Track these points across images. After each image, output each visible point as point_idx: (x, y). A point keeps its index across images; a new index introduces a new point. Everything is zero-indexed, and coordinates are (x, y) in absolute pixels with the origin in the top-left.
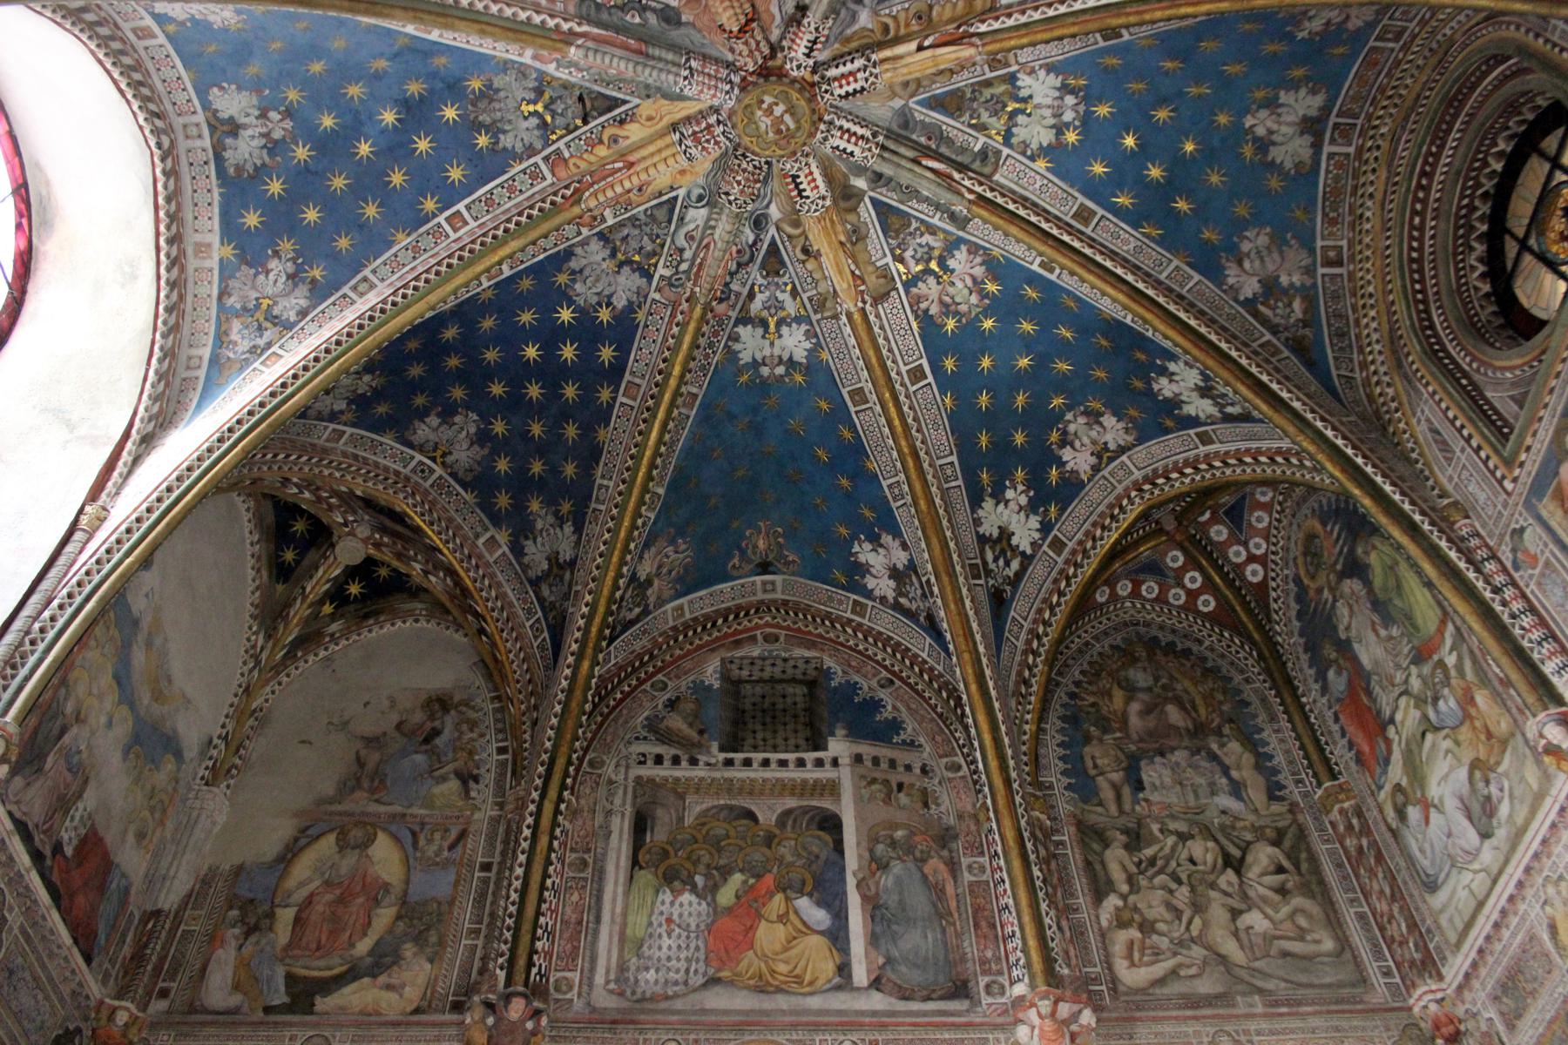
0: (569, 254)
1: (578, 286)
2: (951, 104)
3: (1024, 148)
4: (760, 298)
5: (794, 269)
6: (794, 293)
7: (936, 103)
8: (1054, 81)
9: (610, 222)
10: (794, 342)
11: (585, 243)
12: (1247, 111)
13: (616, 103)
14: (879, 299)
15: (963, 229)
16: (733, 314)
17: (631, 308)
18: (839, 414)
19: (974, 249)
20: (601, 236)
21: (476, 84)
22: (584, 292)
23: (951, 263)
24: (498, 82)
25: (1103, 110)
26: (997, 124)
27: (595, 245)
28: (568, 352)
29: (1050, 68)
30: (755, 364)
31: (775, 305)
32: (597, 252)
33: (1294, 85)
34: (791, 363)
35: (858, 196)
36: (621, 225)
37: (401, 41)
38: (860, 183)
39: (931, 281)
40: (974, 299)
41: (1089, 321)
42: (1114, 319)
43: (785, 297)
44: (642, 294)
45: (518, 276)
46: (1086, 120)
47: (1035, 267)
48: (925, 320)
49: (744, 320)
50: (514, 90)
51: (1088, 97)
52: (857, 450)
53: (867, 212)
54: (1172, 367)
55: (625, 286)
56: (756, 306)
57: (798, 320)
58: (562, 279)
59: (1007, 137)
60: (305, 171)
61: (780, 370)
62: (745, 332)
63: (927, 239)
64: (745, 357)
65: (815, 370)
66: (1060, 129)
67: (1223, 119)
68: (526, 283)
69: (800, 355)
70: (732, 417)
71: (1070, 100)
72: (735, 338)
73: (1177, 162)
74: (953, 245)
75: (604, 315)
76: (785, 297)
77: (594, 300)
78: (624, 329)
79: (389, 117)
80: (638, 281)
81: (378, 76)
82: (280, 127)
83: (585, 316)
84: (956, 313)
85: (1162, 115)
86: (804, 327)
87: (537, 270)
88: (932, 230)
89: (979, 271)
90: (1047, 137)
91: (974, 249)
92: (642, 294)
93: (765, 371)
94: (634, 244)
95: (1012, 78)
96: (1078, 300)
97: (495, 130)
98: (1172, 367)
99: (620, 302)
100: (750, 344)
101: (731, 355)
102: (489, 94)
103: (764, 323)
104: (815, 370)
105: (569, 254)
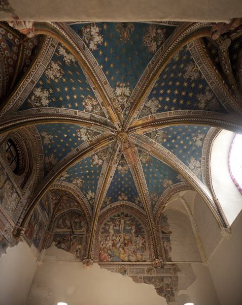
0: (158, 111)
1: (157, 104)
2: (96, 134)
3: (84, 129)
4: (125, 101)
5: (118, 106)
6: (119, 101)
7: (99, 133)
8: (83, 139)
9: (149, 116)
10: (119, 91)
11: (155, 113)
12: (54, 138)
13: (146, 135)
14: (102, 102)
15: (91, 115)
16: (130, 99)
17: (148, 101)
18: (109, 77)
19: (88, 111)
20: (152, 114)
21: (165, 140)
22: (156, 103)
23: (92, 107)
24: (162, 140)
25: (74, 135)
26: (89, 131)
27: (153, 112)
28: (162, 92)
29: (83, 141)
30: (126, 86)
31: (122, 99)
32: (153, 110)
33: (49, 144)
34: (119, 86)
35: (109, 119)
36: (148, 115)
37: (172, 151)
38: (109, 121)
39: (94, 104)
40: (86, 101)
41: (64, 103)
42: (60, 107)
43: (120, 100)
44: (146, 103)
45: (167, 111)
46: (76, 133)
47: (77, 111)
48: (95, 98)
49: (128, 97)
50: (160, 139)
51: (77, 137)
52: (104, 70)
53: (107, 116)
54: (48, 101)
55: (149, 104)
56: (126, 99)
57: (118, 96)
58: (160, 106)
59: (87, 130)
60: (193, 133)
61: (121, 85)
62: (128, 94)
63: (97, 112)
64: (128, 89)
65: (114, 86)
66: (79, 131)
67: (56, 136)
68: (166, 108)
69: (117, 88)
70: (131, 75)
71: (79, 136)
72: (130, 93)
73: (60, 130)
74: (92, 111)
75: (154, 99)
76: (120, 100)
77: (155, 101)
78: (150, 97)
79: (178, 137)
80: (146, 105)
81: (178, 144)
82: (194, 139)
83: (157, 98)
84: (89, 98)
85: (65, 136)
86: (117, 95)
87: (164, 110)
88: (96, 113)
89: (87, 107)
90: (81, 130)
91: (88, 111)
92: (146, 103)
93: (124, 85)
94: (146, 111)
95: (88, 139)
96: (68, 107)
97: (164, 133)
98: (48, 101)
99: (150, 101)
100: (127, 91)
101: (130, 90)
102: (163, 138)
103: (124, 95)
104: (114, 86)
105: (158, 111)
